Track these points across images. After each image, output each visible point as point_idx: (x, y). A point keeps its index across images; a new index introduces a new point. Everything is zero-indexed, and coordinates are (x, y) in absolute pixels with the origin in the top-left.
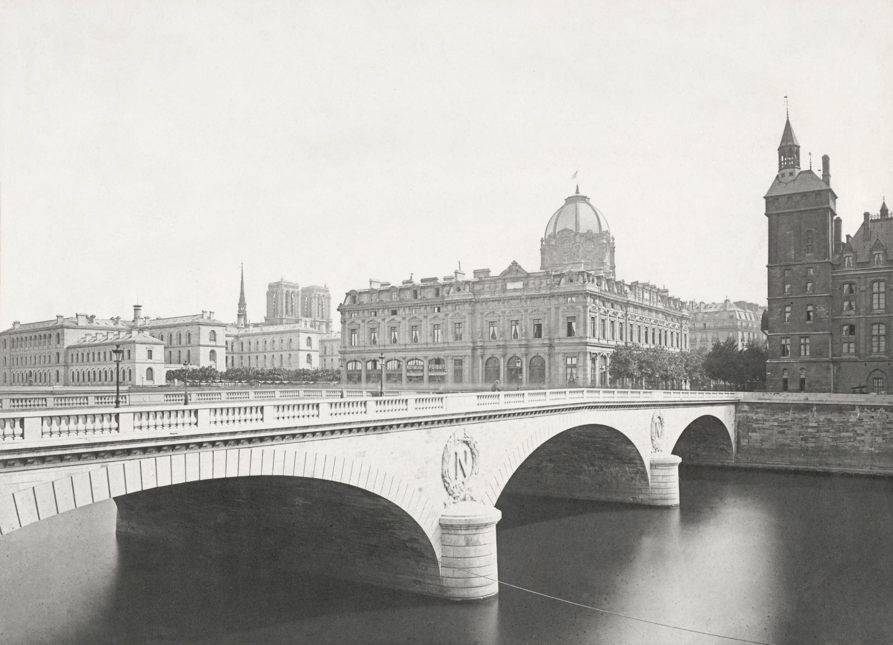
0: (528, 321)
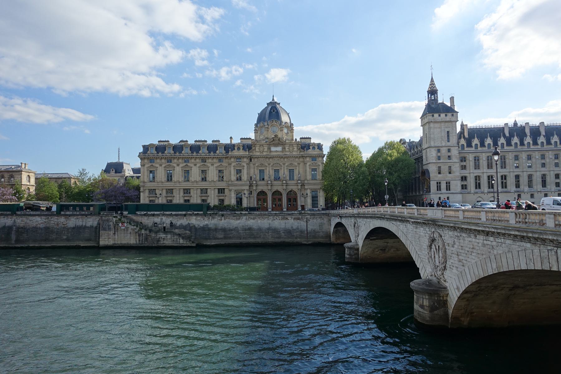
0: (286, 170)
